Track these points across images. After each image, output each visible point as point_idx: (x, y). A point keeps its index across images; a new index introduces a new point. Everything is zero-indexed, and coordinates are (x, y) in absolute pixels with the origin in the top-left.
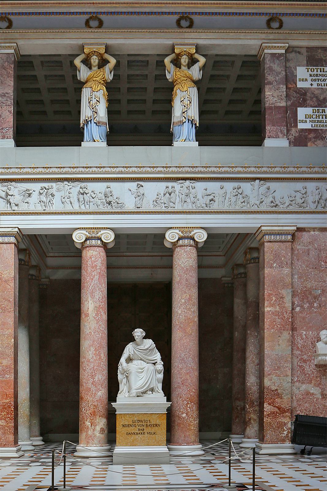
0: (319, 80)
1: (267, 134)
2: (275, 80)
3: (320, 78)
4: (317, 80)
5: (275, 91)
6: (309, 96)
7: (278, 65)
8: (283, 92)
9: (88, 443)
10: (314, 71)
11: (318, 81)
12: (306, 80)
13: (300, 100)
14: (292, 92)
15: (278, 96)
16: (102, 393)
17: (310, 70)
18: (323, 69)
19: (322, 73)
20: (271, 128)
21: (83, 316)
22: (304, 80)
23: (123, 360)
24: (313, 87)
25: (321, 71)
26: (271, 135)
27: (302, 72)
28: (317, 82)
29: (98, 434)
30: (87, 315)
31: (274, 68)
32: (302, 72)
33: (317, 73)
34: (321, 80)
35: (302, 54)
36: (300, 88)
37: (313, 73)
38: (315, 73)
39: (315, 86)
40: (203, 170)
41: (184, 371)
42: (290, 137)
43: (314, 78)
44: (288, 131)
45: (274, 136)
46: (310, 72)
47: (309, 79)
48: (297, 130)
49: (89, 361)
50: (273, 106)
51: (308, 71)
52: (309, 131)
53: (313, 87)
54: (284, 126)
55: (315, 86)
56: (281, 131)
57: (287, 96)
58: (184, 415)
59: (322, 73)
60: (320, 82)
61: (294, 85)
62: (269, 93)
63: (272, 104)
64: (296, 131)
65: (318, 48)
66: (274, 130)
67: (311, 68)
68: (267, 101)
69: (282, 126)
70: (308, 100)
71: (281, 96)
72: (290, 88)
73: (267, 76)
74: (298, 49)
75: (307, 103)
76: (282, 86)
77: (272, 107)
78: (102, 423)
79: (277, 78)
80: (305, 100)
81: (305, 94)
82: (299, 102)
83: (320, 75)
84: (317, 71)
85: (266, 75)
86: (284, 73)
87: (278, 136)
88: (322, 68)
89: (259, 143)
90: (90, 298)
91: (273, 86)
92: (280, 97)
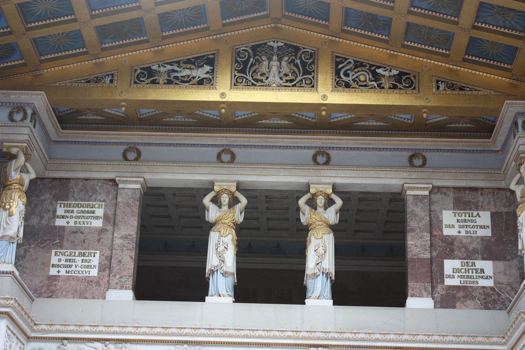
0: (468, 227)
1: (410, 292)
2: (418, 227)
3: (469, 224)
4: (465, 227)
5: (418, 240)
6: (457, 245)
7: (421, 209)
8: (427, 241)
10: (461, 216)
11: (467, 228)
12: (453, 226)
13: (446, 250)
14: (436, 241)
15: (421, 246)
17: (457, 215)
18: (472, 213)
19: (471, 218)
20: (414, 285)
22: (451, 226)
24: (461, 234)
25: (469, 216)
26: (413, 294)
28: (465, 229)
31: (417, 212)
33: (465, 218)
34: (470, 227)
35: (449, 196)
36: (447, 236)
37: (461, 218)
38: (463, 218)
39: (463, 233)
40: (336, 335)
42: (436, 295)
43: (462, 224)
44: (433, 288)
45: (418, 295)
46: (457, 217)
47: (457, 225)
48: (444, 288)
50: (416, 257)
51: (455, 216)
52: (457, 288)
53: (461, 234)
54: (429, 282)
55: (463, 233)
56: (425, 289)
57: (431, 245)
59: (471, 218)
60: (468, 229)
61: (440, 232)
62: (411, 242)
63: (415, 256)
64: (443, 289)
66: (417, 287)
67: (458, 212)
68: (409, 252)
69: (426, 282)
70: (456, 250)
71: (425, 245)
72: (435, 236)
73: (410, 222)
75: (454, 254)
76: (426, 234)
77: (415, 259)
79: (421, 224)
80: (452, 251)
81: (452, 243)
82: (445, 253)
83: (468, 220)
84: (465, 216)
85: (408, 220)
86: (428, 218)
87: (422, 295)
88: (471, 212)
89: (402, 304)
91: (416, 234)
92: (424, 247)
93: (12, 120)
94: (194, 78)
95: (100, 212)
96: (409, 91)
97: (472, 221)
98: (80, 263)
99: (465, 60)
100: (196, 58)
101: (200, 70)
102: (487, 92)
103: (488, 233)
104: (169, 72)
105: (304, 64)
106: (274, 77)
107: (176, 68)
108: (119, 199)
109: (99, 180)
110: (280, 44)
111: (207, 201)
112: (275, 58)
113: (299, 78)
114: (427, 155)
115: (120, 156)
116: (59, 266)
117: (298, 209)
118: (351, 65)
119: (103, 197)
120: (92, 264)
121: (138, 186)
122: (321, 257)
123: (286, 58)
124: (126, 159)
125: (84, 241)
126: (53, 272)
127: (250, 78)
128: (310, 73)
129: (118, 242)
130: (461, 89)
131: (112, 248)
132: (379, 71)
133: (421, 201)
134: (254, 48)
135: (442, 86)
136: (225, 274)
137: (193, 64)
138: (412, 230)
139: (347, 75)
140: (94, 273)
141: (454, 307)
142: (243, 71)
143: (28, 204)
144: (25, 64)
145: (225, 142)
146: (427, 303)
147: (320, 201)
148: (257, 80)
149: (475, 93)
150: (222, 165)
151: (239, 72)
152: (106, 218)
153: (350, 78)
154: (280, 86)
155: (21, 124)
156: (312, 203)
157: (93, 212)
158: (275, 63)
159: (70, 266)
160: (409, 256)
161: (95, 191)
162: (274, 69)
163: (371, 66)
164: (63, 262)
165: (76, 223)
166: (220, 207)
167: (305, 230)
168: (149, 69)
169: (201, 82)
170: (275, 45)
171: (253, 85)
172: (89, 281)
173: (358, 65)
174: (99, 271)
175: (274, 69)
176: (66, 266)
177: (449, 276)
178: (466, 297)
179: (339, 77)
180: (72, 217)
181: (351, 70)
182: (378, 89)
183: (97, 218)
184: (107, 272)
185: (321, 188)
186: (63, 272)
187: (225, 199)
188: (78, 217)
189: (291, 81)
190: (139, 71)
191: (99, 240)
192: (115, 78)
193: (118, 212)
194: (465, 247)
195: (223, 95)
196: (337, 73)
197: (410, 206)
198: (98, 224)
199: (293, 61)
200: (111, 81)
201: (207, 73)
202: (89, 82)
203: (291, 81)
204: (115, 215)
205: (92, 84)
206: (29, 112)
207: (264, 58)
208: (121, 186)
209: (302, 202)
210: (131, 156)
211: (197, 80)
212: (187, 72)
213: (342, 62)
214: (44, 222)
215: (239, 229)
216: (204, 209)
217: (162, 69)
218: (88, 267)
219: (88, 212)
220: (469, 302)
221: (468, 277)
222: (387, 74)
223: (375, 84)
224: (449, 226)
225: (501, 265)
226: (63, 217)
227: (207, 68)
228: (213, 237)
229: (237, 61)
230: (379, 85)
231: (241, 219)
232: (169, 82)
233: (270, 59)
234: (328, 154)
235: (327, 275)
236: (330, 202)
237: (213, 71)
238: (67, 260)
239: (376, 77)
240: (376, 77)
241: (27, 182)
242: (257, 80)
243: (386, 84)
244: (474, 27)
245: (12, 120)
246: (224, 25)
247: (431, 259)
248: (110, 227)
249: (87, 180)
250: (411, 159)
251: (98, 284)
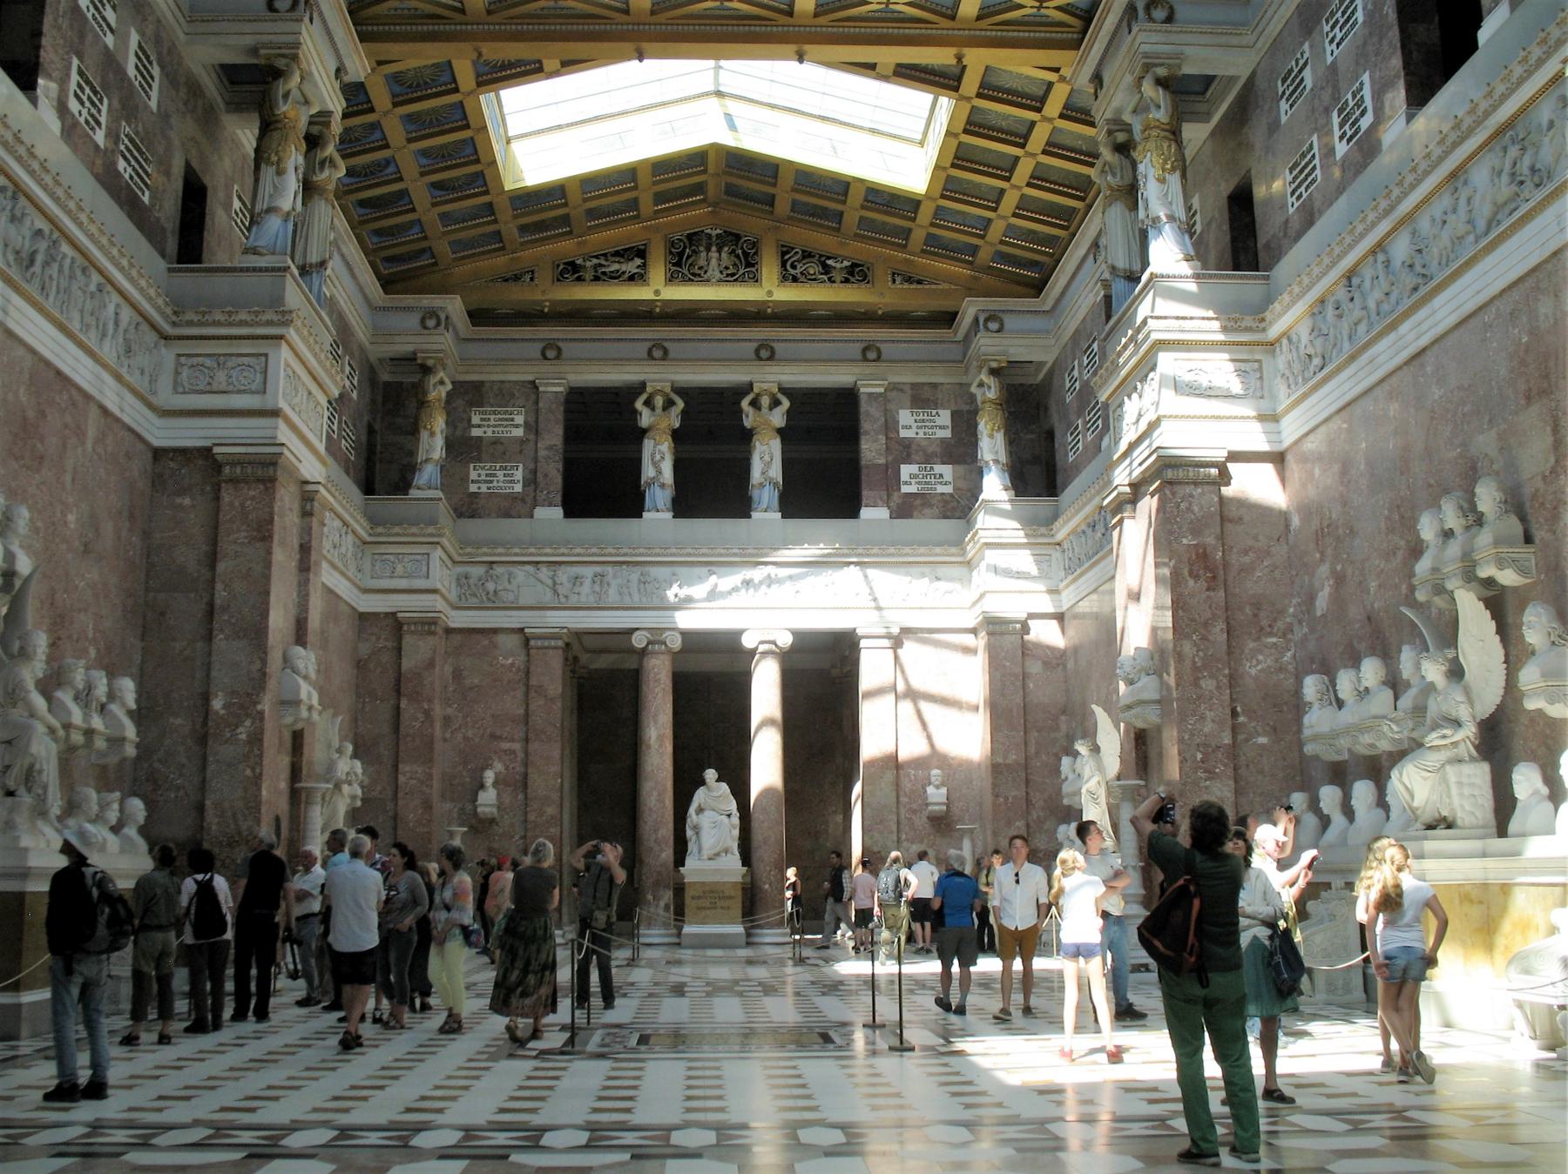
9: (650, 924)
16: (667, 854)
21: (644, 748)
23: (692, 810)
27: (905, 417)
29: (661, 912)
30: (649, 747)
32: (905, 417)
38: (921, 417)
39: (921, 435)
41: (766, 824)
44: (889, 496)
47: (914, 425)
49: (650, 809)
57: (887, 449)
58: (767, 886)
65: (923, 384)
74: (901, 386)
78: (667, 896)
80: (909, 455)
89: (853, 513)
90: (652, 724)
93: (425, 327)
94: (624, 273)
95: (520, 419)
96: (863, 285)
97: (931, 421)
98: (501, 478)
99: (923, 251)
100: (625, 250)
101: (630, 263)
102: (946, 286)
103: (947, 434)
104: (596, 267)
105: (744, 253)
106: (714, 271)
107: (603, 262)
108: (541, 405)
109: (516, 382)
110: (718, 231)
111: (639, 405)
112: (714, 248)
113: (741, 271)
114: (883, 347)
115: (539, 355)
116: (478, 482)
117: (741, 411)
118: (799, 256)
119: (521, 401)
120: (515, 478)
121: (561, 389)
122: (769, 464)
123: (726, 249)
124: (545, 358)
125: (504, 453)
126: (473, 488)
127: (686, 272)
128: (753, 265)
129: (542, 453)
130: (919, 282)
131: (536, 460)
132: (830, 262)
133: (876, 399)
134: (690, 237)
135: (898, 279)
136: (663, 486)
137: (622, 256)
138: (867, 433)
139: (794, 267)
140: (518, 488)
141: (910, 516)
142: (678, 264)
143: (447, 423)
144: (435, 264)
145: (657, 336)
146: (882, 513)
147: (765, 401)
148: (694, 275)
149: (934, 287)
150: (654, 362)
151: (674, 265)
152: (527, 425)
153: (798, 271)
154: (720, 281)
155: (436, 331)
156: (755, 404)
157: (512, 420)
158: (714, 254)
159: (491, 482)
160: (863, 462)
161: (512, 395)
162: (714, 262)
163: (821, 256)
164: (483, 477)
165: (494, 432)
166: (653, 409)
167: (747, 436)
168: (572, 264)
169: (632, 278)
170: (714, 233)
171: (691, 280)
172: (514, 498)
173: (807, 255)
174: (524, 486)
175: (714, 262)
176: (486, 482)
177: (906, 483)
178: (923, 505)
179: (786, 270)
180: (489, 426)
181: (797, 261)
182: (829, 284)
183: (517, 426)
184: (533, 487)
185: (765, 386)
186: (484, 488)
187: (659, 401)
188: (495, 426)
189: (733, 275)
190: (561, 267)
191: (521, 451)
192: (536, 275)
193: (541, 418)
194: (924, 451)
195: (657, 292)
196: (784, 264)
197: (864, 406)
198: (519, 432)
199: (734, 251)
200: (532, 279)
201: (639, 267)
202: (507, 280)
203: (733, 275)
204: (537, 421)
205: (511, 284)
206: (443, 317)
207: (701, 249)
208: (541, 389)
209: (745, 403)
210: (551, 354)
211: (627, 275)
212: (615, 267)
213: (787, 253)
214: (459, 433)
215: (677, 436)
216: (635, 413)
217: (588, 264)
218: (511, 482)
219: (506, 420)
220: (927, 511)
221: (927, 483)
222: (838, 265)
223: (825, 277)
224: (905, 427)
225: (961, 469)
226: (479, 426)
227: (638, 261)
228: (648, 445)
229: (671, 253)
230: (829, 279)
231: (677, 425)
232: (596, 279)
233: (708, 250)
234: (772, 348)
235: (776, 484)
236: (776, 403)
237: (644, 266)
238: (487, 475)
239: (827, 269)
240: (827, 269)
241: (444, 395)
242: (694, 275)
243: (838, 278)
244: (932, 225)
245: (425, 327)
246: (657, 212)
247: (886, 466)
248: (532, 437)
249: (503, 382)
250: (865, 350)
251: (523, 500)
